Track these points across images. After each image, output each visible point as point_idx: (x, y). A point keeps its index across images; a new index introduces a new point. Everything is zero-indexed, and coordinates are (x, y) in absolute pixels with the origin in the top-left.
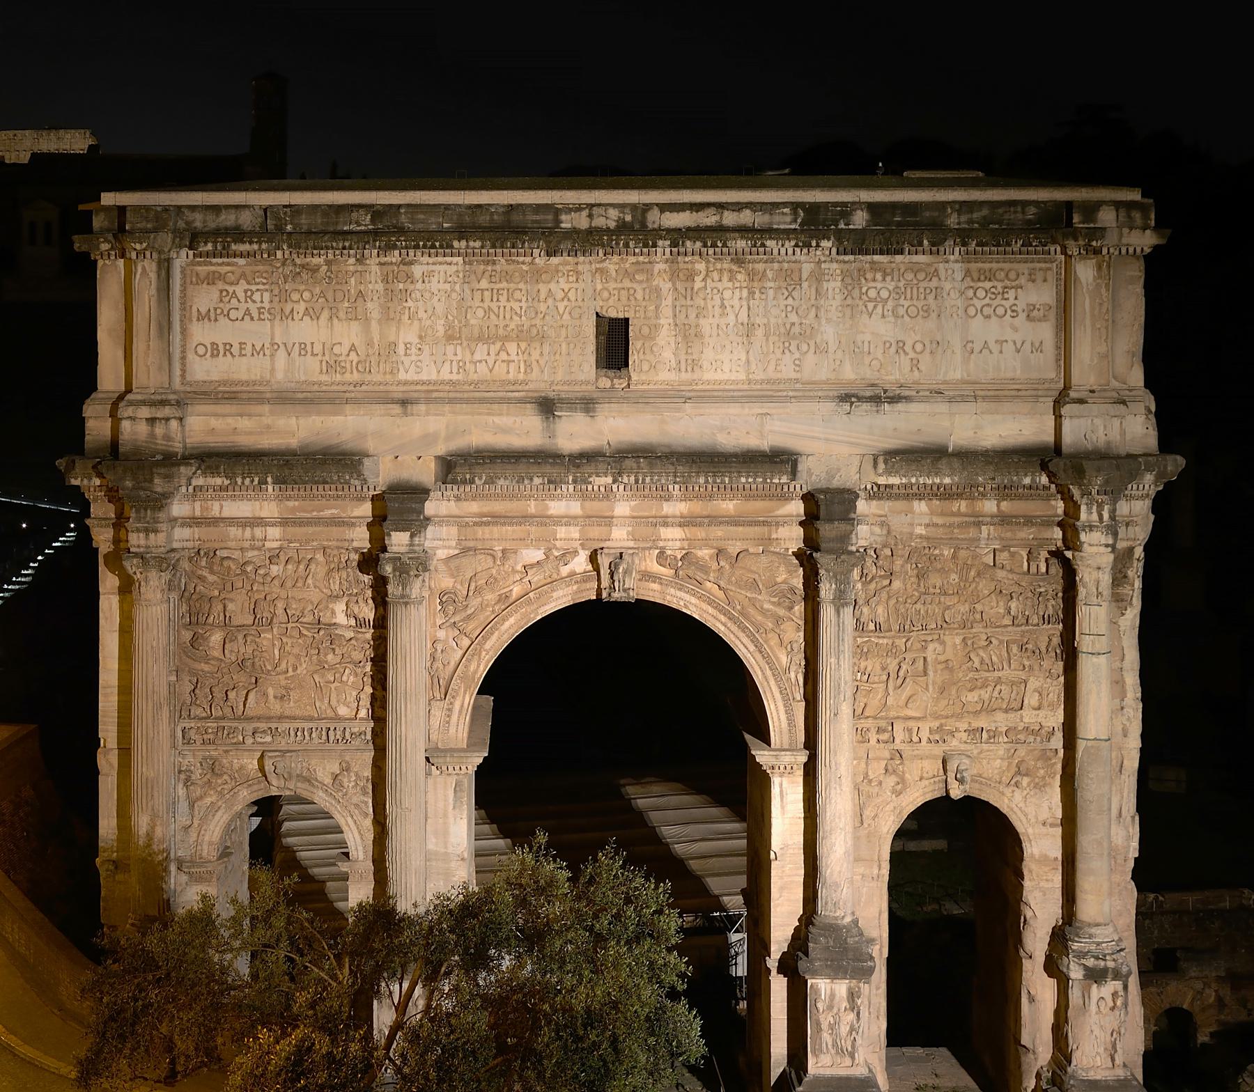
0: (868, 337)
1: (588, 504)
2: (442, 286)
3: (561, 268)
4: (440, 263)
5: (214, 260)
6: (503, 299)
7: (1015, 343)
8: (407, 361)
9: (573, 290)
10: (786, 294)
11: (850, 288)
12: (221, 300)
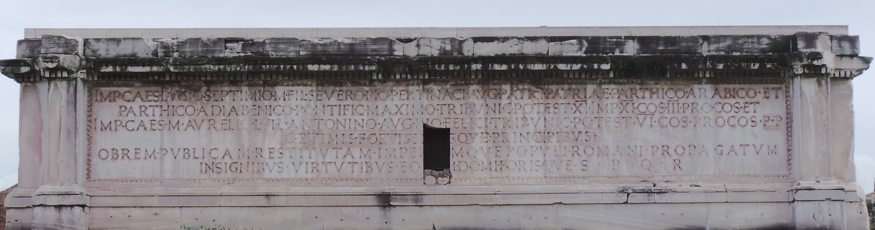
2: (299, 103)
3: (395, 88)
4: (298, 85)
5: (115, 83)
6: (349, 113)
7: (754, 146)
8: (271, 163)
9: (404, 108)
10: (575, 108)
11: (625, 103)
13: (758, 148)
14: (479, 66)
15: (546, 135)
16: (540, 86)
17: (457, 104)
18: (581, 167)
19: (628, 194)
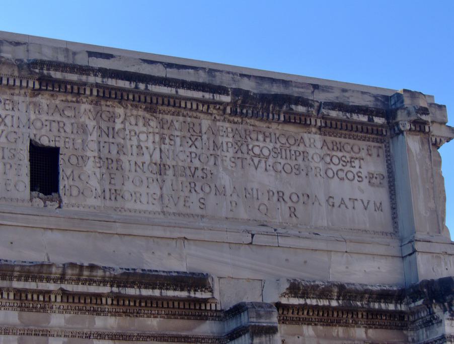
0: (255, 186)
1: (26, 315)
7: (362, 201)
9: (9, 118)
10: (190, 143)
13: (366, 205)
14: (99, 80)
15: (162, 168)
16: (155, 114)
17: (68, 122)
18: (199, 204)
19: (253, 235)
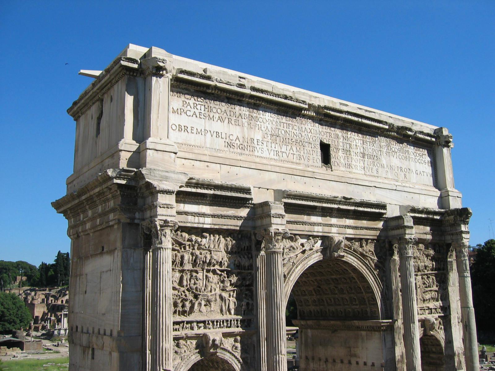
6: (291, 128)
9: (313, 130)
12: (183, 106)
15: (363, 155)
17: (332, 133)
